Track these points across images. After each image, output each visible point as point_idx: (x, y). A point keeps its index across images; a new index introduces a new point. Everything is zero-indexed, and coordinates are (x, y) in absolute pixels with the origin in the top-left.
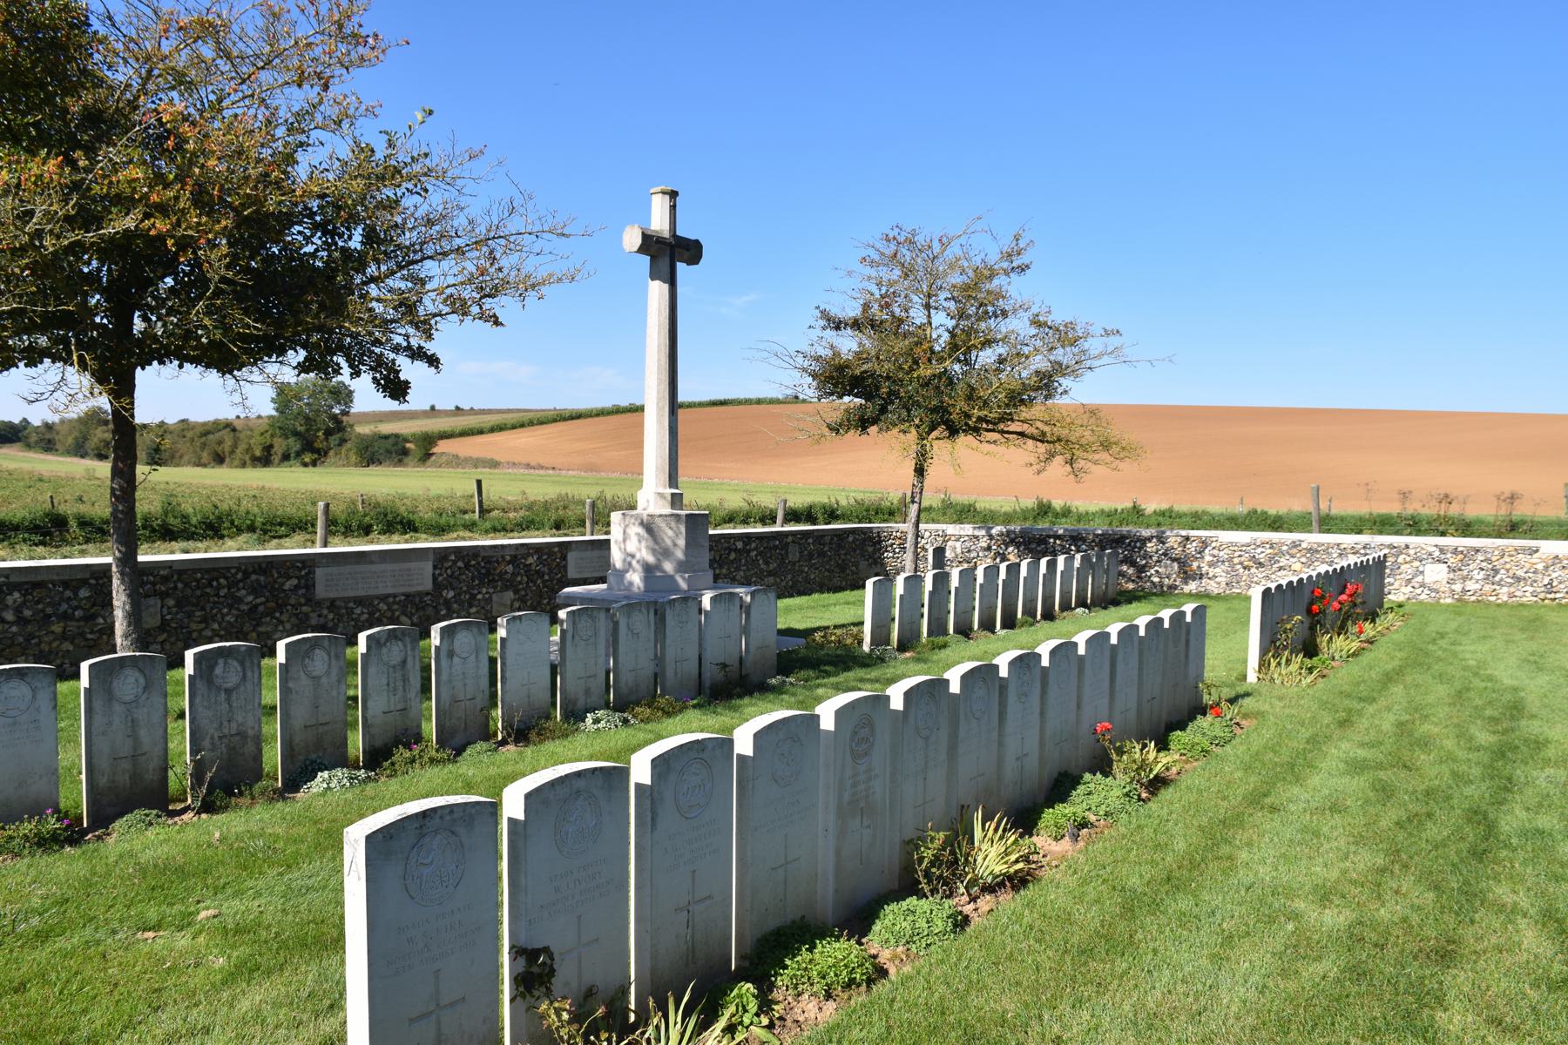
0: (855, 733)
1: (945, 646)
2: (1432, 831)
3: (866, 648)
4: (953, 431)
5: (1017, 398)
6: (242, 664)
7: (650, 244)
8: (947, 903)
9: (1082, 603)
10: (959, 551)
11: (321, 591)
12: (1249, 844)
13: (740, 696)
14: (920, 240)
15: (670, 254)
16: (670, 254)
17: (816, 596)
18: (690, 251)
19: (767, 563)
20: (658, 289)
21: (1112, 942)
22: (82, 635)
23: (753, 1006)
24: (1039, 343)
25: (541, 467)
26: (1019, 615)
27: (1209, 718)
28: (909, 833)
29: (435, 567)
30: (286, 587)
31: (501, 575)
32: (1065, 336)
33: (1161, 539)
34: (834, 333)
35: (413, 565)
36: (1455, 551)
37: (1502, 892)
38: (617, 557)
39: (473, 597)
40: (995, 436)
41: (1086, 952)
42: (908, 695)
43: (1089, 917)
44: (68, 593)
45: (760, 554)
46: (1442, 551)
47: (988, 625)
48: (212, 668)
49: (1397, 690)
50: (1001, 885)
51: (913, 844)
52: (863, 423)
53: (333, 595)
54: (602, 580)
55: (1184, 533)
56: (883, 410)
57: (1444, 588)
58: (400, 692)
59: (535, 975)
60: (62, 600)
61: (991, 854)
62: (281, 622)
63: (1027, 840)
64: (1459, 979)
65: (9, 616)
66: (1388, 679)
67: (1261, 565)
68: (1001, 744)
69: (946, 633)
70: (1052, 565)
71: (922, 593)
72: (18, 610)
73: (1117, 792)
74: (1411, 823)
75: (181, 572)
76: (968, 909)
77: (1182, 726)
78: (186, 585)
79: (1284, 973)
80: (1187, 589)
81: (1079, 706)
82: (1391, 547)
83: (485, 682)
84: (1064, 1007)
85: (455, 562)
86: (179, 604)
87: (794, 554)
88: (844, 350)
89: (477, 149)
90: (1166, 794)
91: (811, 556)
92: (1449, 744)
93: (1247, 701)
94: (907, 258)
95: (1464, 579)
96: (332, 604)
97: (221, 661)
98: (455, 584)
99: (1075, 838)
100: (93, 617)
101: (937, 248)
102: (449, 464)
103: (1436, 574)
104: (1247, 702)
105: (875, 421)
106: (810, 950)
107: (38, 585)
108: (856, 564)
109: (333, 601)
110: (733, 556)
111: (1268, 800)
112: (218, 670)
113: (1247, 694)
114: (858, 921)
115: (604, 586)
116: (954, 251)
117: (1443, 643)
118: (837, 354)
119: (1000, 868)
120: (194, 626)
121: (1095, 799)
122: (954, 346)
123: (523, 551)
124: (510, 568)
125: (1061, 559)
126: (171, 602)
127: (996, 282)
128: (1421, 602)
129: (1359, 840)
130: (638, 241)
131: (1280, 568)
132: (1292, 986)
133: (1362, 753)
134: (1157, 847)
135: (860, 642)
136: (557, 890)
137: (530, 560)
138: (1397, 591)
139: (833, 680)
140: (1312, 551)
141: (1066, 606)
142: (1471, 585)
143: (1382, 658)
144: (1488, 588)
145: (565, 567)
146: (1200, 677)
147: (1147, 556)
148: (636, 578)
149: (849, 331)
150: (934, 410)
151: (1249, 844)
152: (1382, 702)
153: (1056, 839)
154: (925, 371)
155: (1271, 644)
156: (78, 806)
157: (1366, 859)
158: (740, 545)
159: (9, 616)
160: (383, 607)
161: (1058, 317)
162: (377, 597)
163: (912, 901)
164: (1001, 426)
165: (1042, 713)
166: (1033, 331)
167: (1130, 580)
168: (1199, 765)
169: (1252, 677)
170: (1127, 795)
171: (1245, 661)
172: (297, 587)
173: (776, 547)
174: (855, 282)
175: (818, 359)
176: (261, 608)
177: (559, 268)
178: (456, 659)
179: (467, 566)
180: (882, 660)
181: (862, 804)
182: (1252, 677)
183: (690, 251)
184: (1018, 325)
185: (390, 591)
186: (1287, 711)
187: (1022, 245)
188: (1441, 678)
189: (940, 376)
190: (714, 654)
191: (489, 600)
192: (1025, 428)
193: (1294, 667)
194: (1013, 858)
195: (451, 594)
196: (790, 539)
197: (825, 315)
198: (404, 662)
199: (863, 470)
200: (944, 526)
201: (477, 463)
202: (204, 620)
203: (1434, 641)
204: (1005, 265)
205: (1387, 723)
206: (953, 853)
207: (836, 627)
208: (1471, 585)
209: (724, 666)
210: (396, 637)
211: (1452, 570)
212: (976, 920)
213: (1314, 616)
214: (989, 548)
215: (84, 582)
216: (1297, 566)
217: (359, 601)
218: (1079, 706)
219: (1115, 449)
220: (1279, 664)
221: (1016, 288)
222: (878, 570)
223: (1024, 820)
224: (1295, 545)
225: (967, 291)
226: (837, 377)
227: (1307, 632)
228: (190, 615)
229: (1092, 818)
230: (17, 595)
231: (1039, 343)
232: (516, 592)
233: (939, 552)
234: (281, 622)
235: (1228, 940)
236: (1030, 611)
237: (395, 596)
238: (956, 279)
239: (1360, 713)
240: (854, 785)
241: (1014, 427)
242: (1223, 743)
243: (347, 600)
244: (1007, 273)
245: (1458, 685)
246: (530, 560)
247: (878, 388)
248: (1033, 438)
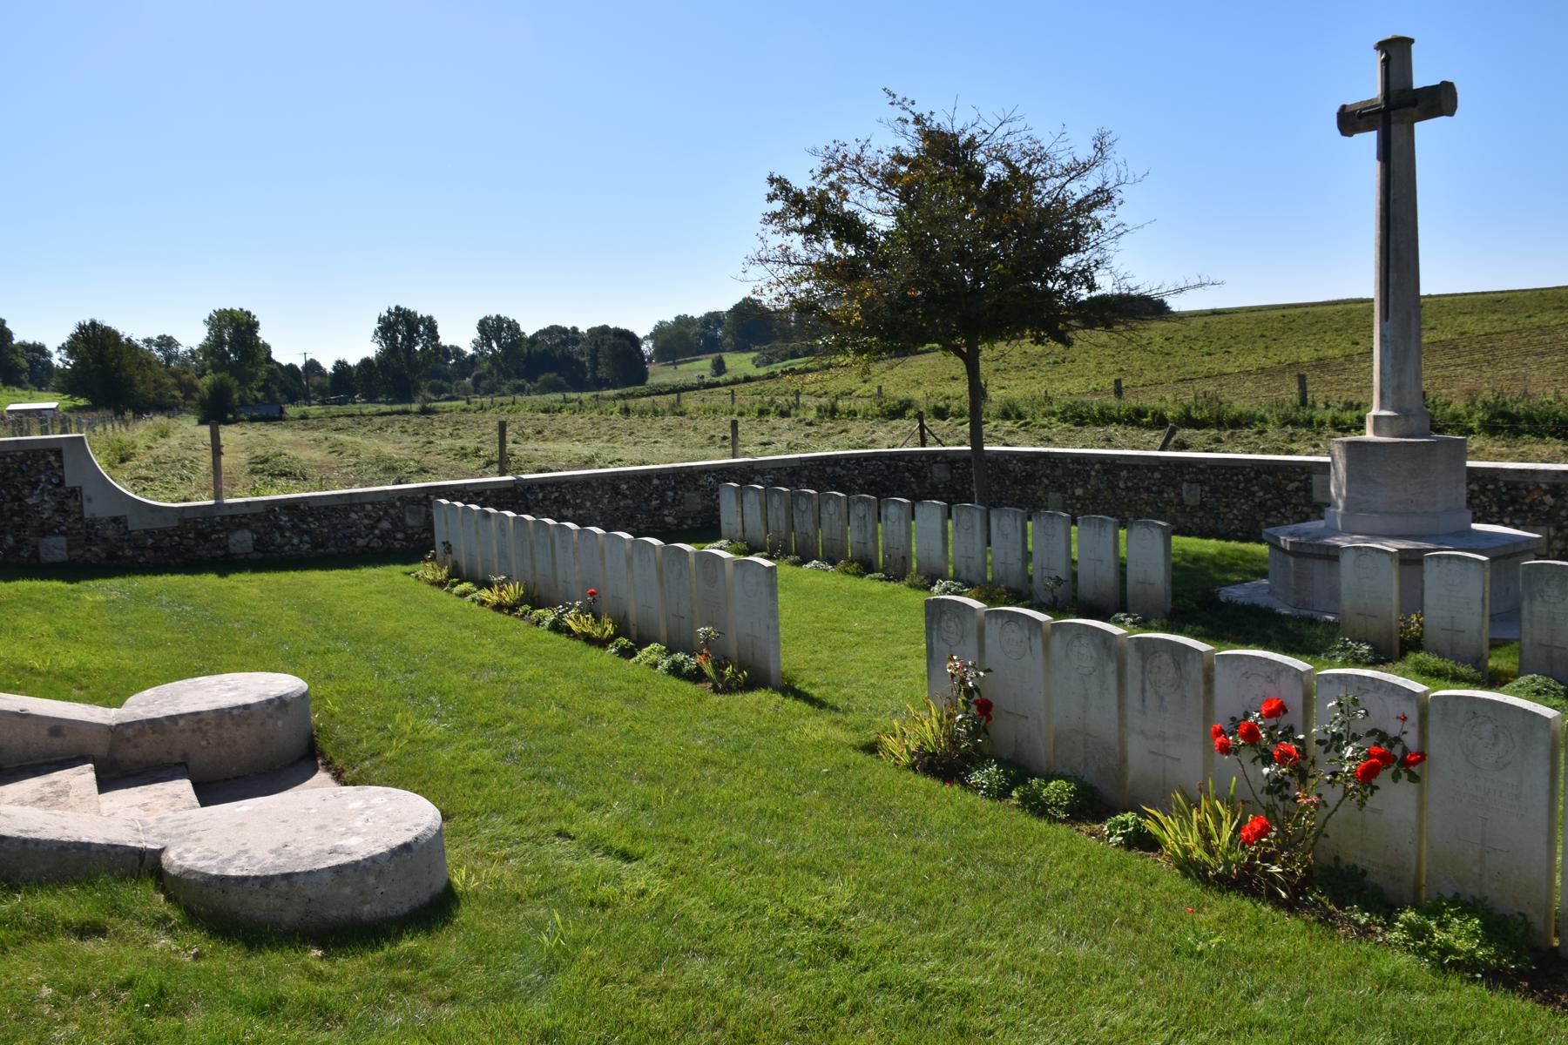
18: (1441, 100)
30: (1291, 487)
83: (939, 545)
107: (1136, 467)
124: (1549, 499)
159: (1122, 485)
172: (1298, 489)
183: (1441, 100)
215: (1156, 468)
228: (1218, 500)
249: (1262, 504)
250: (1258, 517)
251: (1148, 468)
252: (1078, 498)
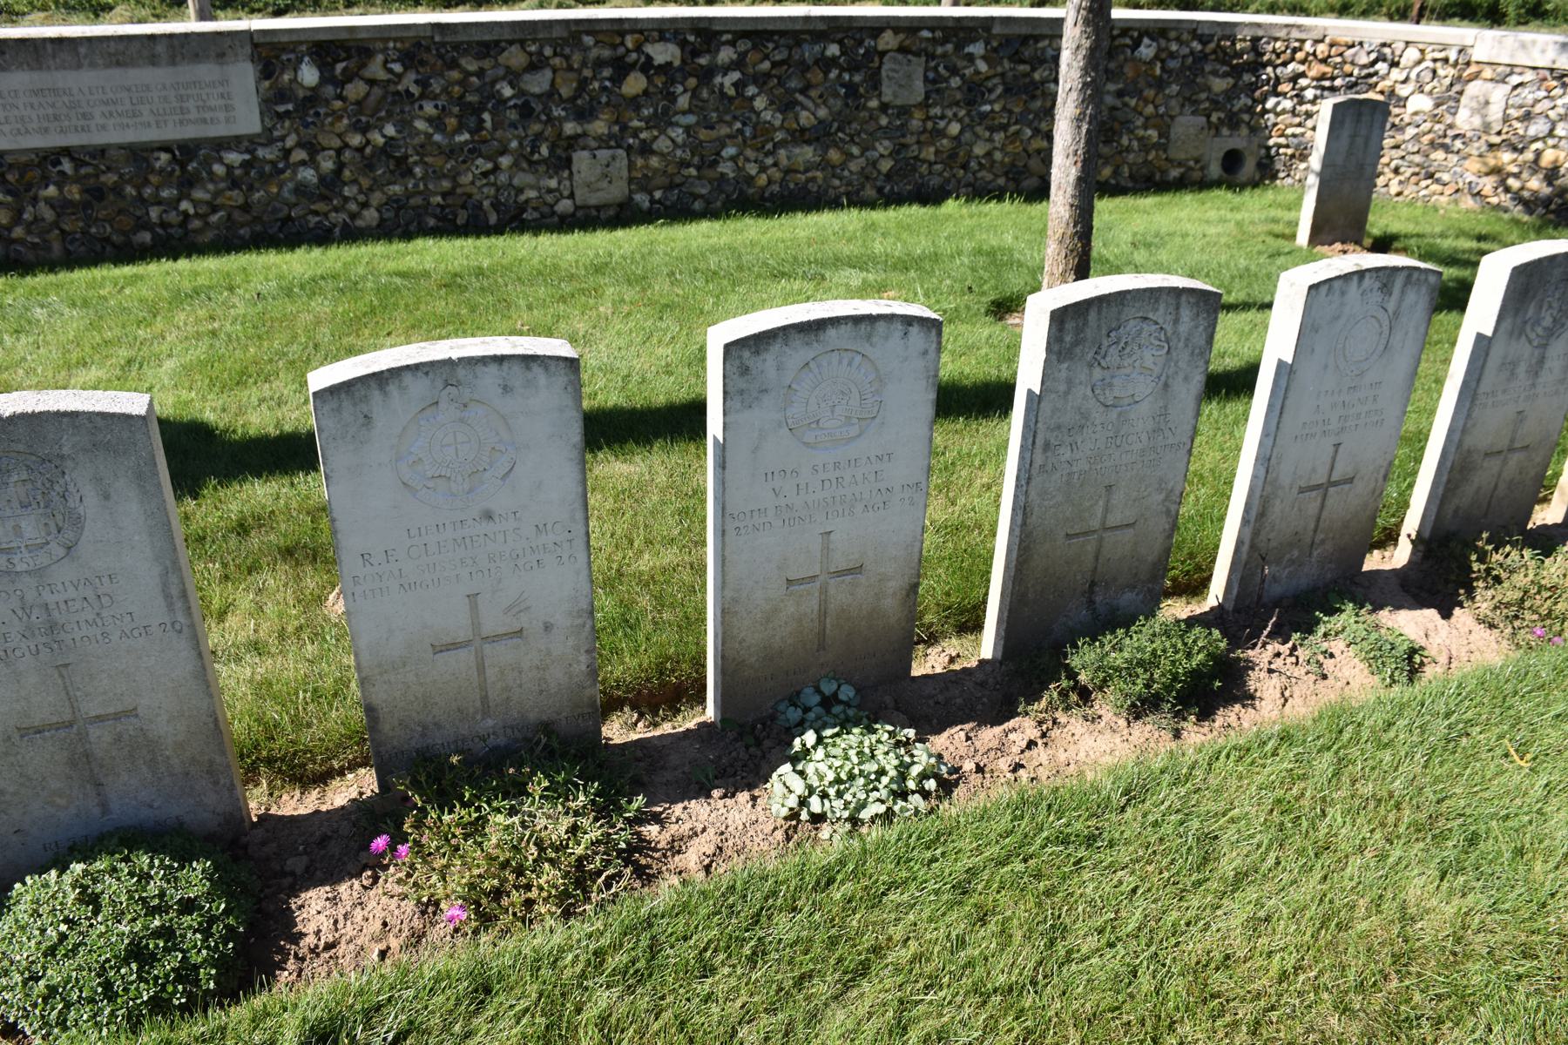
10: (1495, 112)
19: (787, 106)
45: (761, 80)
87: (904, 83)
91: (975, 91)
110: (634, 84)
158: (663, 53)
173: (826, 64)
196: (888, 40)
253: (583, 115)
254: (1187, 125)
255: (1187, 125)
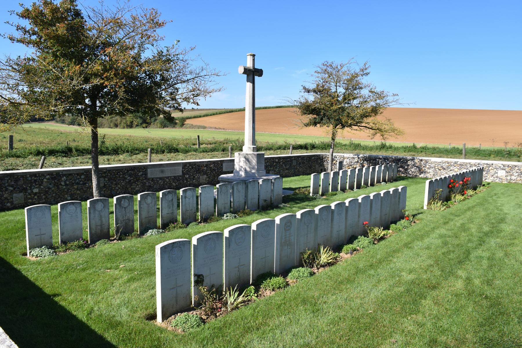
0: (286, 224)
1: (336, 194)
2: (452, 256)
3: (311, 195)
4: (343, 127)
5: (365, 115)
6: (129, 200)
7: (246, 71)
8: (309, 269)
9: (384, 180)
11: (149, 176)
12: (398, 257)
13: (270, 210)
14: (334, 65)
15: (253, 74)
16: (253, 74)
17: (301, 176)
18: (260, 72)
19: (286, 166)
20: (249, 85)
21: (349, 280)
22: (82, 189)
23: (253, 291)
24: (372, 98)
25: (220, 129)
26: (362, 184)
27: (404, 220)
28: (302, 251)
29: (183, 168)
30: (139, 174)
31: (203, 170)
32: (380, 96)
33: (413, 160)
34: (307, 94)
35: (176, 168)
36: (508, 166)
37: (460, 273)
38: (237, 167)
39: (194, 177)
40: (356, 127)
41: (341, 283)
42: (320, 210)
43: (346, 274)
44: (78, 177)
45: (284, 163)
46: (504, 166)
47: (351, 188)
48: (121, 202)
49: (469, 213)
50: (326, 265)
51: (302, 254)
52: (315, 123)
53: (153, 177)
54: (231, 172)
55: (420, 158)
56: (322, 119)
57: (504, 178)
58: (171, 208)
59: (199, 280)
60: (77, 179)
61: (324, 257)
62: (138, 185)
63: (337, 254)
64: (434, 293)
65: (63, 183)
66: (469, 209)
67: (444, 169)
68: (332, 227)
69: (337, 190)
70: (374, 169)
71: (329, 179)
72: (65, 182)
73: (367, 241)
74: (449, 252)
75: (109, 171)
76: (316, 271)
77: (395, 223)
78: (111, 174)
79: (390, 290)
80: (420, 176)
81: (359, 217)
82: (487, 164)
83: (195, 205)
84: (330, 295)
85: (189, 167)
86: (109, 180)
87: (294, 163)
88: (309, 101)
89: (193, 47)
90: (382, 242)
91: (300, 164)
92: (473, 230)
93: (420, 215)
94: (330, 71)
95: (511, 175)
96: (153, 179)
97: (123, 200)
98: (189, 173)
99: (352, 254)
100: (85, 184)
101: (339, 67)
102: (190, 127)
103: (502, 173)
104: (420, 216)
105: (319, 123)
106: (270, 279)
108: (315, 166)
109: (153, 179)
110: (275, 164)
111: (410, 245)
112: (122, 202)
113: (422, 213)
114: (285, 273)
115: (232, 175)
116: (345, 69)
117: (494, 198)
118: (307, 102)
119: (325, 261)
120: (113, 186)
121: (360, 243)
122: (345, 99)
123: (210, 163)
124: (205, 168)
125: (377, 167)
126: (107, 179)
127: (359, 78)
128: (496, 183)
129: (430, 257)
130: (243, 71)
131: (451, 170)
132: (389, 293)
133: (445, 232)
134: (372, 257)
135: (309, 193)
136: (205, 261)
137: (211, 166)
138: (488, 178)
139: (298, 205)
140: (460, 165)
141: (379, 182)
142: (513, 178)
143: (471, 202)
144: (519, 178)
145: (222, 168)
146: (404, 208)
147: (408, 165)
148: (243, 174)
149: (312, 93)
150: (338, 120)
151: (398, 257)
152: (462, 216)
153: (346, 254)
154: (335, 107)
155: (432, 198)
156: (87, 238)
157: (430, 262)
158: (277, 160)
159: (63, 183)
160: (167, 180)
161: (378, 90)
162: (166, 177)
163: (301, 268)
164: (359, 125)
165: (346, 219)
166: (370, 94)
167: (402, 173)
168: (395, 235)
169: (425, 208)
170: (370, 242)
171: (423, 202)
172: (142, 174)
174: (313, 78)
175: (301, 103)
176: (132, 181)
177: (216, 87)
178: (187, 199)
179: (192, 168)
180: (315, 199)
181: (288, 243)
182: (425, 208)
183: (260, 72)
184: (365, 92)
185: (170, 175)
186: (431, 219)
187: (367, 67)
188: (485, 210)
189: (340, 108)
190: (263, 196)
191: (199, 178)
192: (366, 125)
193: (439, 204)
194: (329, 258)
195: (188, 176)
197: (304, 88)
198: (172, 200)
199: (320, 134)
200: (343, 154)
201: (199, 127)
202: (116, 184)
203: (491, 197)
204: (361, 73)
205: (458, 224)
206: (313, 256)
207: (303, 188)
208: (513, 178)
209: (265, 201)
210: (170, 193)
211: (507, 172)
212: (317, 274)
213: (446, 190)
214: (358, 162)
215: (83, 174)
216: (456, 170)
217: (161, 178)
218: (359, 217)
219: (396, 132)
220: (434, 204)
221: (364, 80)
222: (322, 168)
223: (337, 248)
224: (456, 163)
225: (350, 80)
226: (307, 109)
227: (448, 193)
228: (112, 183)
229: (358, 248)
230: (65, 177)
231: (372, 98)
232: (207, 175)
233: (341, 163)
234: (138, 185)
235: (379, 281)
236: (366, 184)
237: (171, 177)
238: (345, 77)
239: (452, 220)
240: (285, 238)
241: (363, 125)
242: (405, 227)
243: (157, 178)
244: (362, 75)
245: (489, 212)
246: (211, 166)
247: (320, 112)
248: (368, 128)
249: (130, 181)
250: (128, 186)
251: (78, 174)
252: (35, 194)
253: (271, 167)
254: (317, 166)
255: (317, 166)
